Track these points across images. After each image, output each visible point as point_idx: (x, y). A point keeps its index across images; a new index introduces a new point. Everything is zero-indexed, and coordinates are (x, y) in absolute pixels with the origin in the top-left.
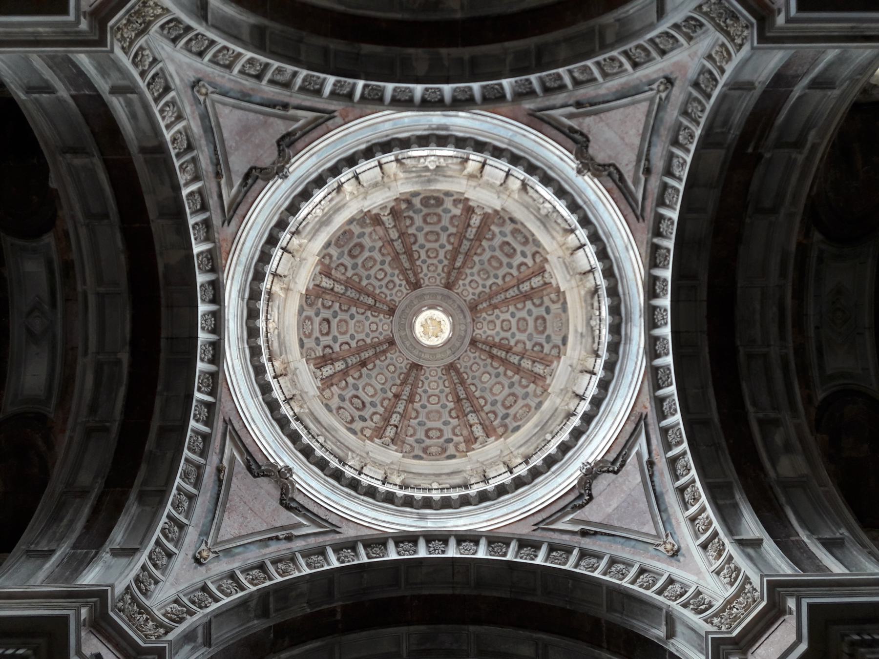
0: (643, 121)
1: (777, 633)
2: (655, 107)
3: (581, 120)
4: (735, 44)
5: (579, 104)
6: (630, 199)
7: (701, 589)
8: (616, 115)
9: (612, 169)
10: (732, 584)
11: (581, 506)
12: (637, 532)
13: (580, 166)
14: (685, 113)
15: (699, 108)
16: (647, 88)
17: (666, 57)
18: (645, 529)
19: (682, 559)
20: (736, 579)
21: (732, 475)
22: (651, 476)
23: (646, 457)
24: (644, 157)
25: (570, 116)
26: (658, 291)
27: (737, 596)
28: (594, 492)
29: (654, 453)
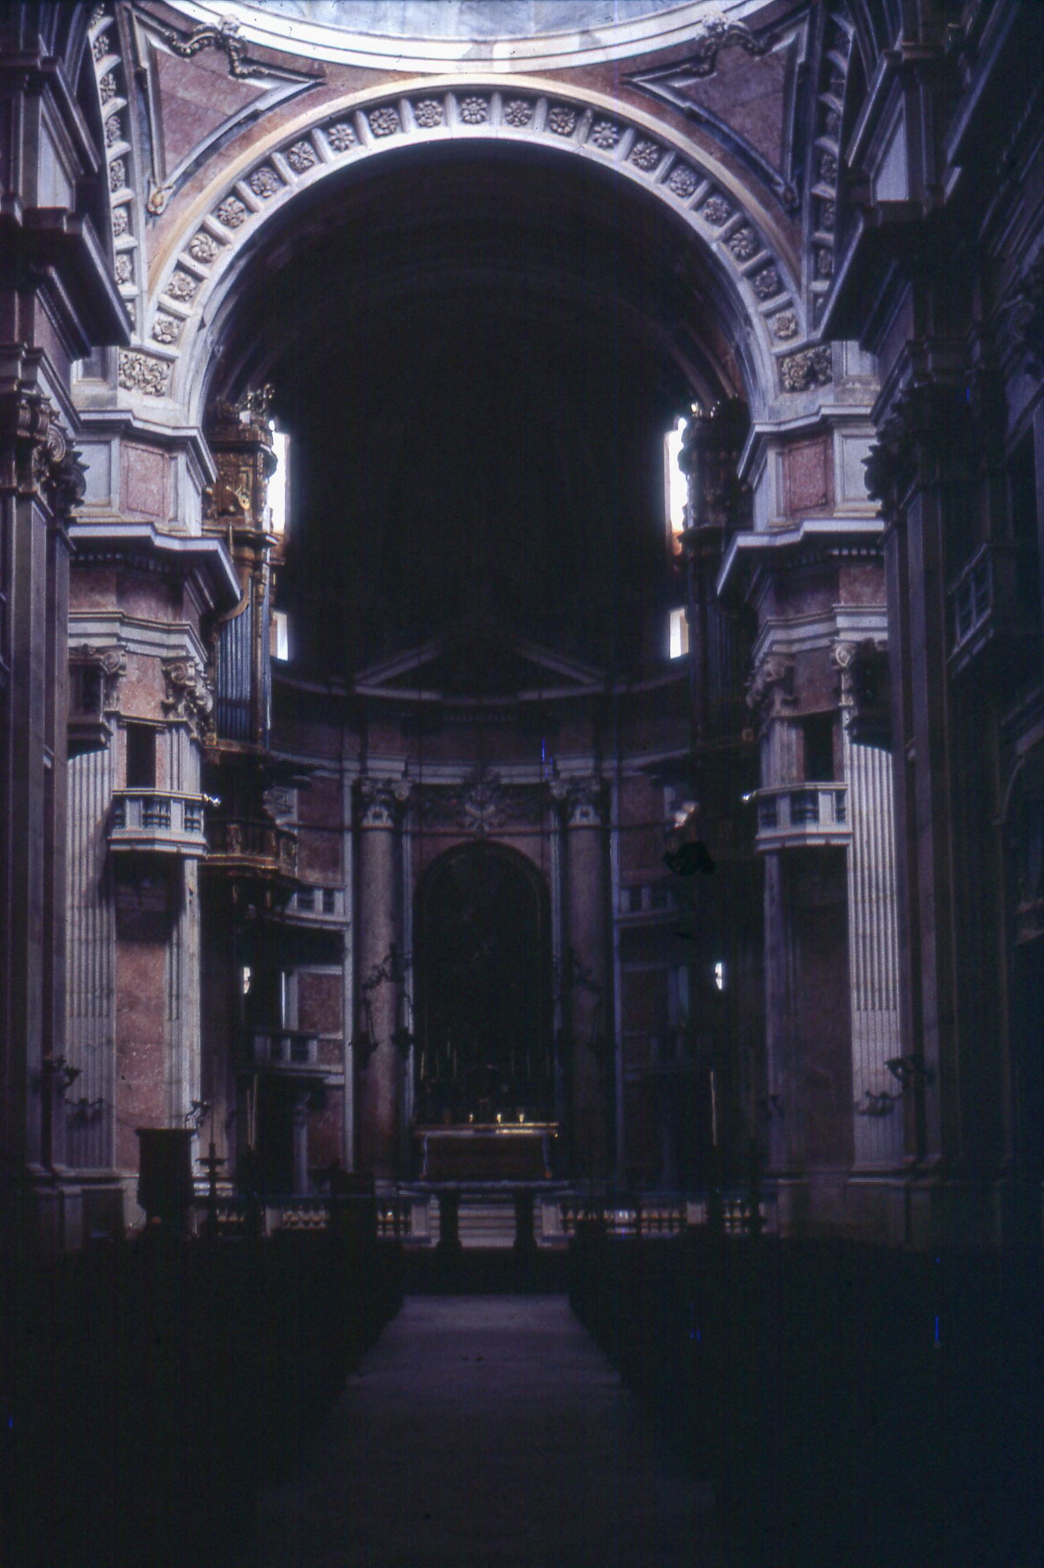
0: (757, 145)
1: (152, 457)
3: (784, 62)
8: (776, 115)
9: (706, 67)
11: (176, 49)
12: (162, 147)
13: (719, 30)
14: (745, 223)
18: (169, 156)
19: (150, 226)
20: (163, 342)
25: (793, 50)
26: (513, 105)
27: (149, 354)
28: (200, 57)
29: (270, 114)
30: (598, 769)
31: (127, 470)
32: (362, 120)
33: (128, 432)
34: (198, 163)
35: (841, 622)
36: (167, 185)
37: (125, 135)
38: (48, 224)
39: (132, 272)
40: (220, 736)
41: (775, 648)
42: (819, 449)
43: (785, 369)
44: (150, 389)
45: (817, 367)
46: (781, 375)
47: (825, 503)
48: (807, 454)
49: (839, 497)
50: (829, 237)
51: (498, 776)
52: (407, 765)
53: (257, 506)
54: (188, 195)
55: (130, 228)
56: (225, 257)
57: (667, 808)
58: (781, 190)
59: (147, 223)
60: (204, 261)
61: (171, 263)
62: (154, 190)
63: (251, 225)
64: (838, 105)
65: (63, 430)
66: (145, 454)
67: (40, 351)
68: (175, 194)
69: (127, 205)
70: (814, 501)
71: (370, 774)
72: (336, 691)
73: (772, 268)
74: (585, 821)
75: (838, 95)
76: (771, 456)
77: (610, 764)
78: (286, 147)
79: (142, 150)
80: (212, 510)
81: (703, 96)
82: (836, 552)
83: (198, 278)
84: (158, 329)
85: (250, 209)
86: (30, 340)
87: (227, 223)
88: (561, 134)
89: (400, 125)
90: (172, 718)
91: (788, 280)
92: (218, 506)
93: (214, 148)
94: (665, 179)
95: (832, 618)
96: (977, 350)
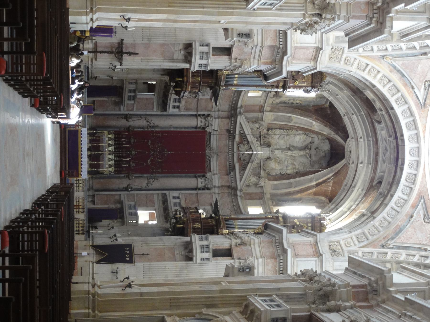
1: (311, 56)
2: (395, 239)
4: (340, 243)
5: (426, 250)
6: (424, 206)
7: (357, 52)
8: (412, 241)
10: (347, 57)
15: (370, 231)
16: (395, 247)
17: (372, 251)
19: (380, 56)
21: (374, 89)
22: (410, 83)
23: (416, 90)
24: (411, 222)
29: (413, 92)
30: (215, 187)
31: (306, 48)
32: (411, 119)
33: (319, 49)
34: (398, 71)
35: (260, 260)
36: (392, 61)
37: (408, 49)
38: (388, 24)
39: (366, 51)
40: (227, 75)
41: (252, 240)
42: (312, 254)
43: (336, 243)
44: (331, 56)
45: (336, 253)
46: (334, 242)
47: (296, 255)
48: (310, 250)
49: (298, 259)
50: (375, 257)
51: (213, 157)
52: (217, 131)
53: (295, 87)
54: (389, 67)
55: (379, 50)
56: (370, 79)
57: (204, 207)
58: (389, 242)
59: (381, 55)
60: (369, 72)
61: (368, 62)
62: (391, 57)
63: (379, 86)
64: (415, 260)
65: (324, 28)
66: (312, 54)
67: (349, 21)
68: (389, 64)
69: (386, 49)
70: (296, 252)
71: (214, 120)
72: (238, 110)
73: (366, 239)
74: (199, 183)
75: (419, 260)
76: (311, 239)
77: (217, 190)
78: (402, 96)
79: (403, 54)
80: (294, 74)
81: (417, 220)
82: (281, 258)
83: (364, 70)
84: (348, 58)
85: (384, 86)
86: (352, 18)
87: (380, 79)
88: (406, 178)
89: (409, 129)
90: (233, 61)
91: (362, 244)
92: (295, 76)
93: (403, 75)
94: (392, 208)
95: (261, 258)
96: (347, 304)
